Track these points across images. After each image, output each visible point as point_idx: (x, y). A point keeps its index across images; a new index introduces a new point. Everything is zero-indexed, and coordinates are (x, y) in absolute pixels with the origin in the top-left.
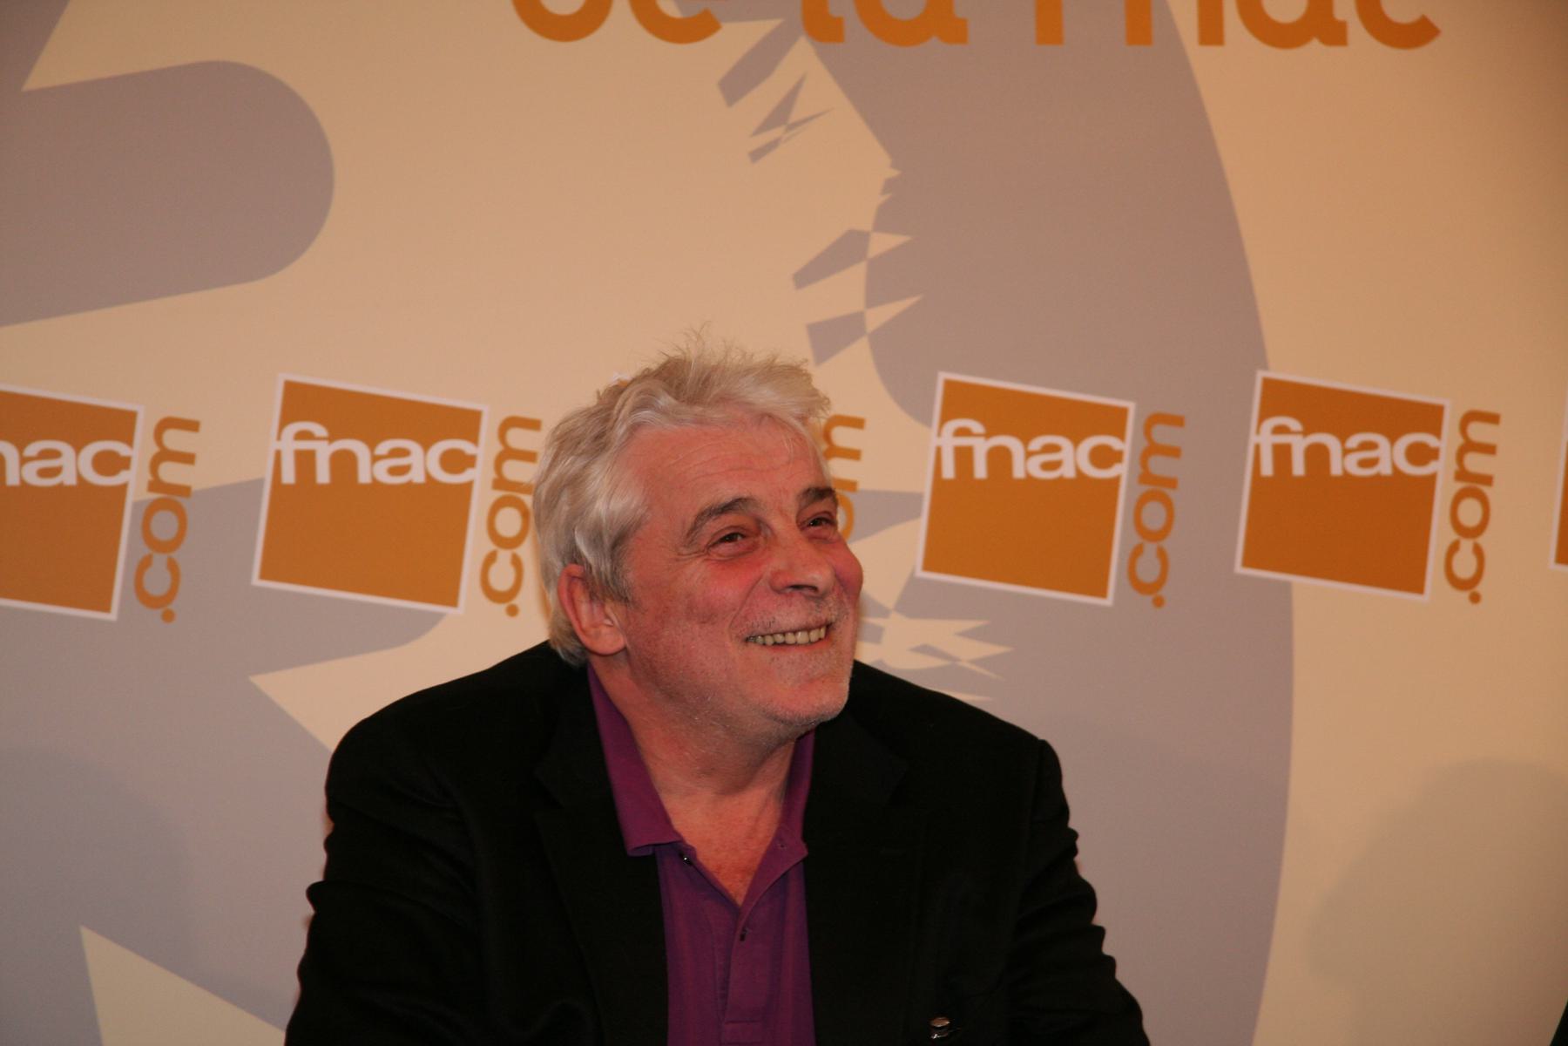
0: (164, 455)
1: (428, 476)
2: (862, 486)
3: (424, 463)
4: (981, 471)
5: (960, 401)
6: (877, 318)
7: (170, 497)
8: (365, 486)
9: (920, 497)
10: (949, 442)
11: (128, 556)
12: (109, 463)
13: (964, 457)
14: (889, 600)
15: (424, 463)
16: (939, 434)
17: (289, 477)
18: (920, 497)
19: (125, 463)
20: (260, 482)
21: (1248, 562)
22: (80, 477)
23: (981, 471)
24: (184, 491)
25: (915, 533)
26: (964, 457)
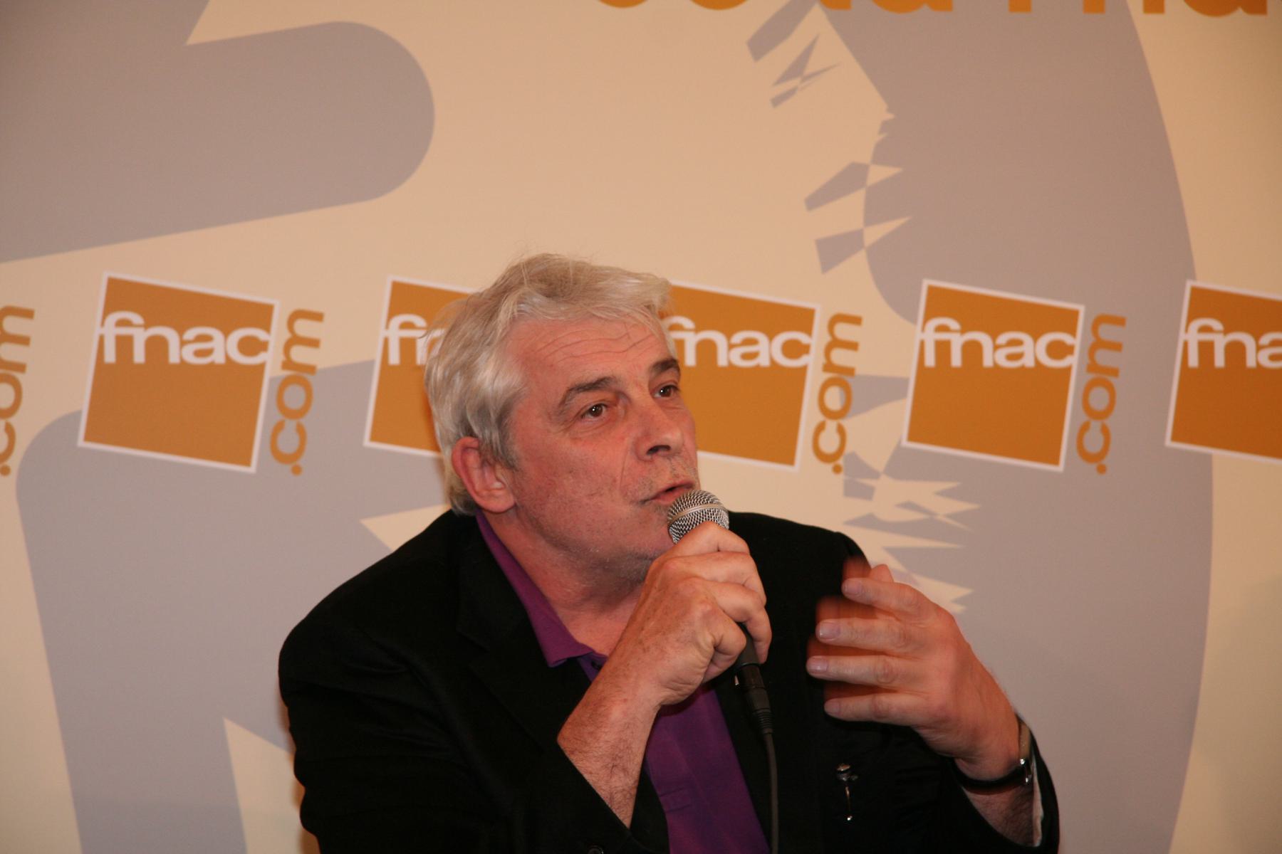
0: (295, 340)
1: (772, 361)
2: (859, 372)
4: (956, 360)
5: (940, 303)
6: (873, 234)
7: (299, 374)
8: (723, 369)
9: (906, 381)
10: (931, 337)
11: (265, 426)
12: (251, 347)
13: (943, 349)
14: (879, 462)
16: (923, 329)
17: (394, 359)
18: (906, 381)
19: (263, 346)
20: (371, 364)
22: (227, 358)
23: (956, 360)
24: (311, 369)
25: (903, 410)
26: (943, 349)
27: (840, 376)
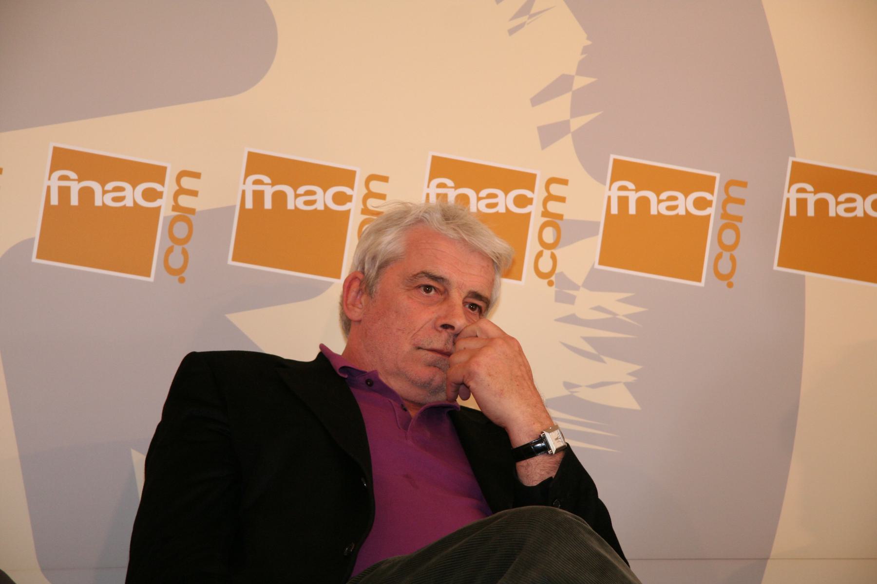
0: (181, 191)
2: (565, 217)
3: (323, 199)
5: (622, 171)
6: (577, 123)
7: (184, 214)
9: (598, 223)
10: (615, 194)
12: (151, 195)
13: (623, 202)
14: (579, 280)
15: (323, 199)
17: (249, 205)
18: (598, 223)
19: (160, 195)
24: (192, 211)
26: (623, 202)
27: (553, 220)
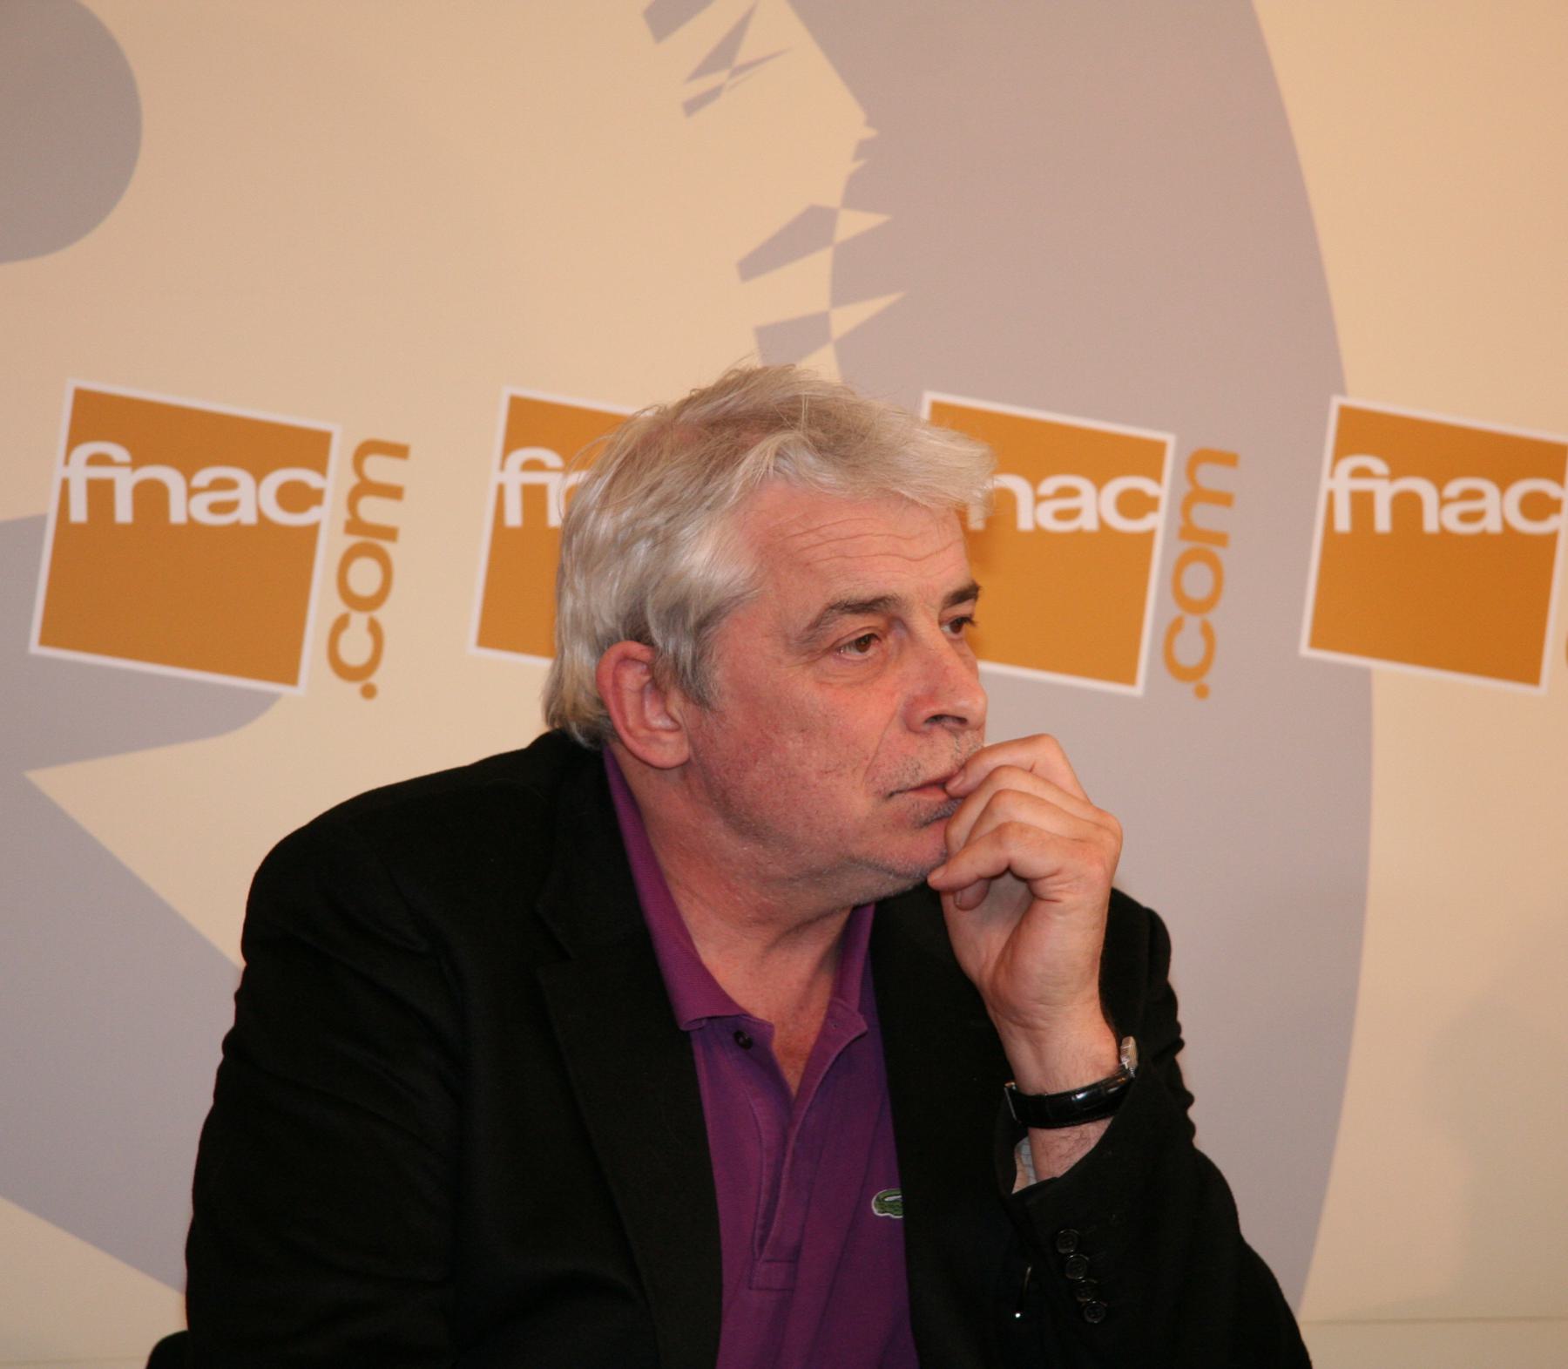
21: (1317, 642)
